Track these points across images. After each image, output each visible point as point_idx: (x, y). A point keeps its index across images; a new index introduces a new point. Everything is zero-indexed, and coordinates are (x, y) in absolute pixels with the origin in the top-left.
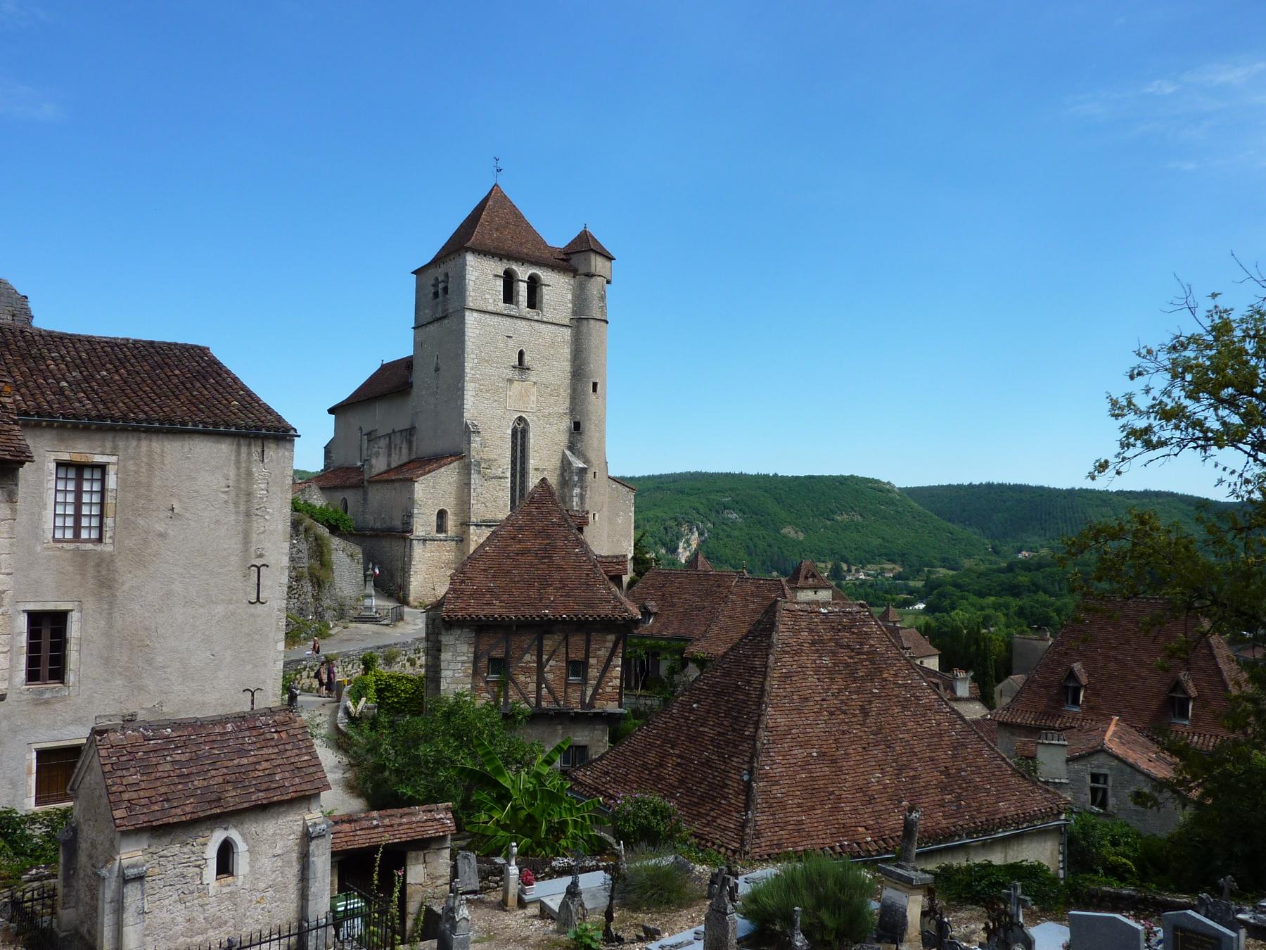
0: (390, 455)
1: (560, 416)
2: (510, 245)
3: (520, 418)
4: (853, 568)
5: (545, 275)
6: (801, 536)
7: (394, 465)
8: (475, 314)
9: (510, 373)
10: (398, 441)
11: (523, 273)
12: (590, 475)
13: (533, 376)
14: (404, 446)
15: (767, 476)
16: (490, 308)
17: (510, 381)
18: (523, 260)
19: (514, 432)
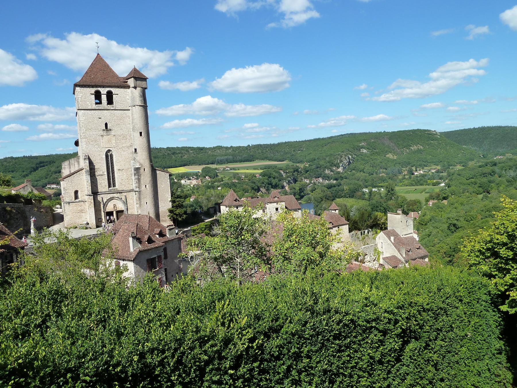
0: (70, 168)
1: (128, 147)
2: (99, 80)
3: (109, 151)
4: (418, 169)
5: (114, 90)
6: (395, 157)
7: (72, 172)
8: (82, 111)
9: (102, 133)
10: (73, 162)
11: (104, 91)
12: (142, 170)
13: (113, 133)
14: (76, 163)
15: (381, 132)
16: (90, 108)
17: (102, 136)
18: (103, 87)
19: (107, 156)
